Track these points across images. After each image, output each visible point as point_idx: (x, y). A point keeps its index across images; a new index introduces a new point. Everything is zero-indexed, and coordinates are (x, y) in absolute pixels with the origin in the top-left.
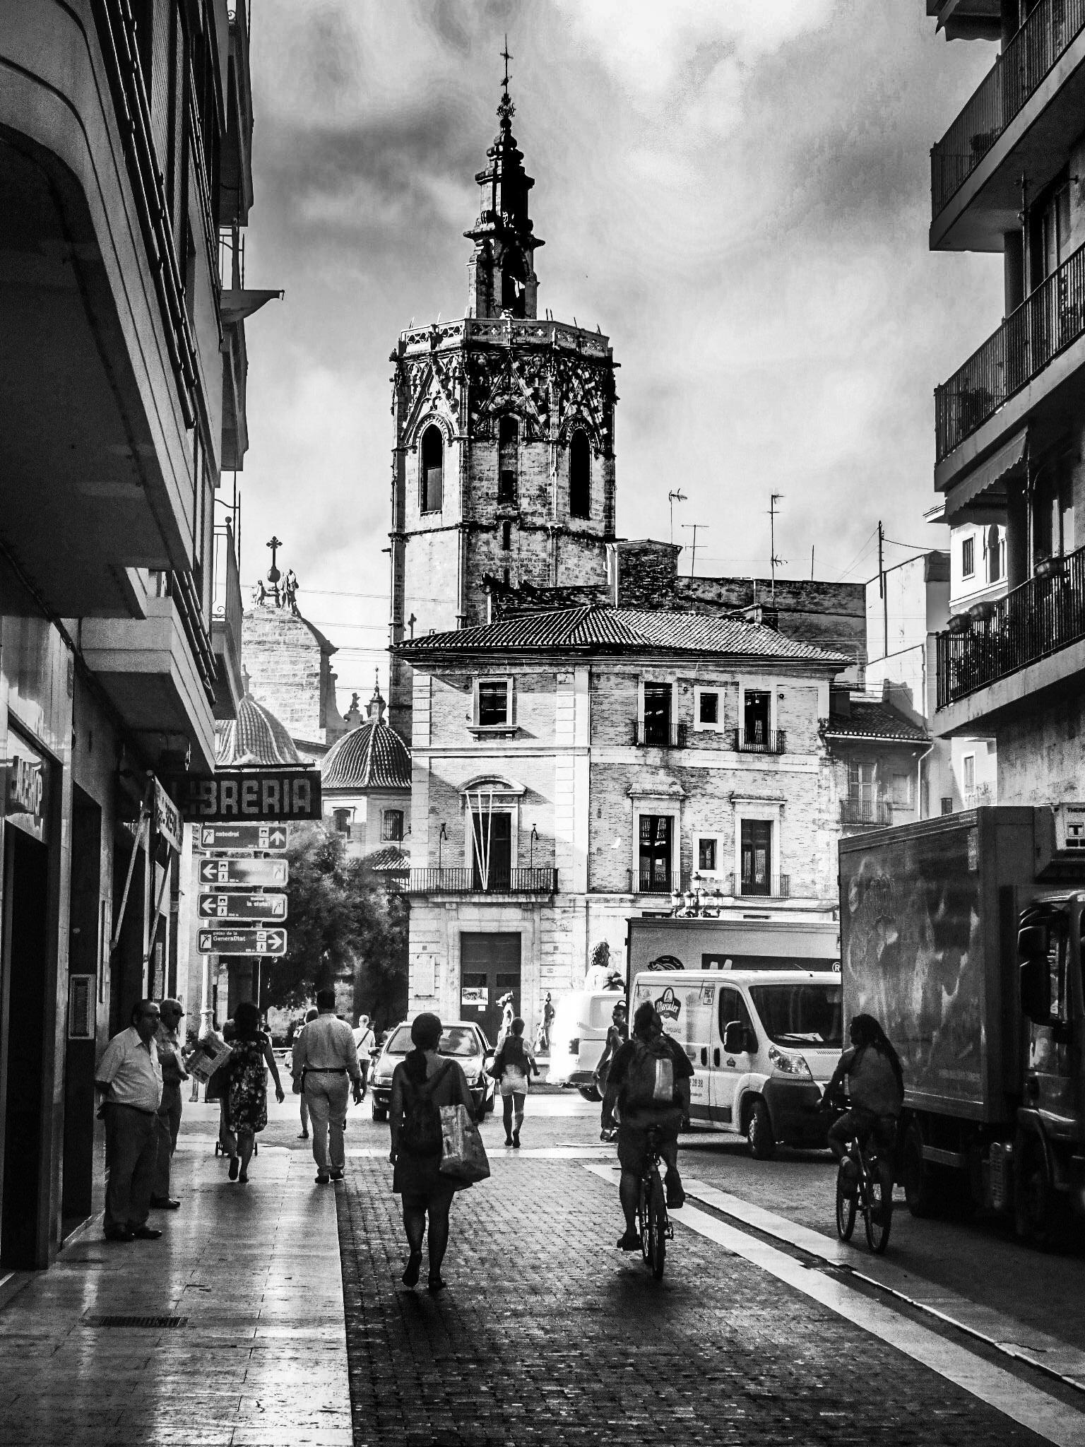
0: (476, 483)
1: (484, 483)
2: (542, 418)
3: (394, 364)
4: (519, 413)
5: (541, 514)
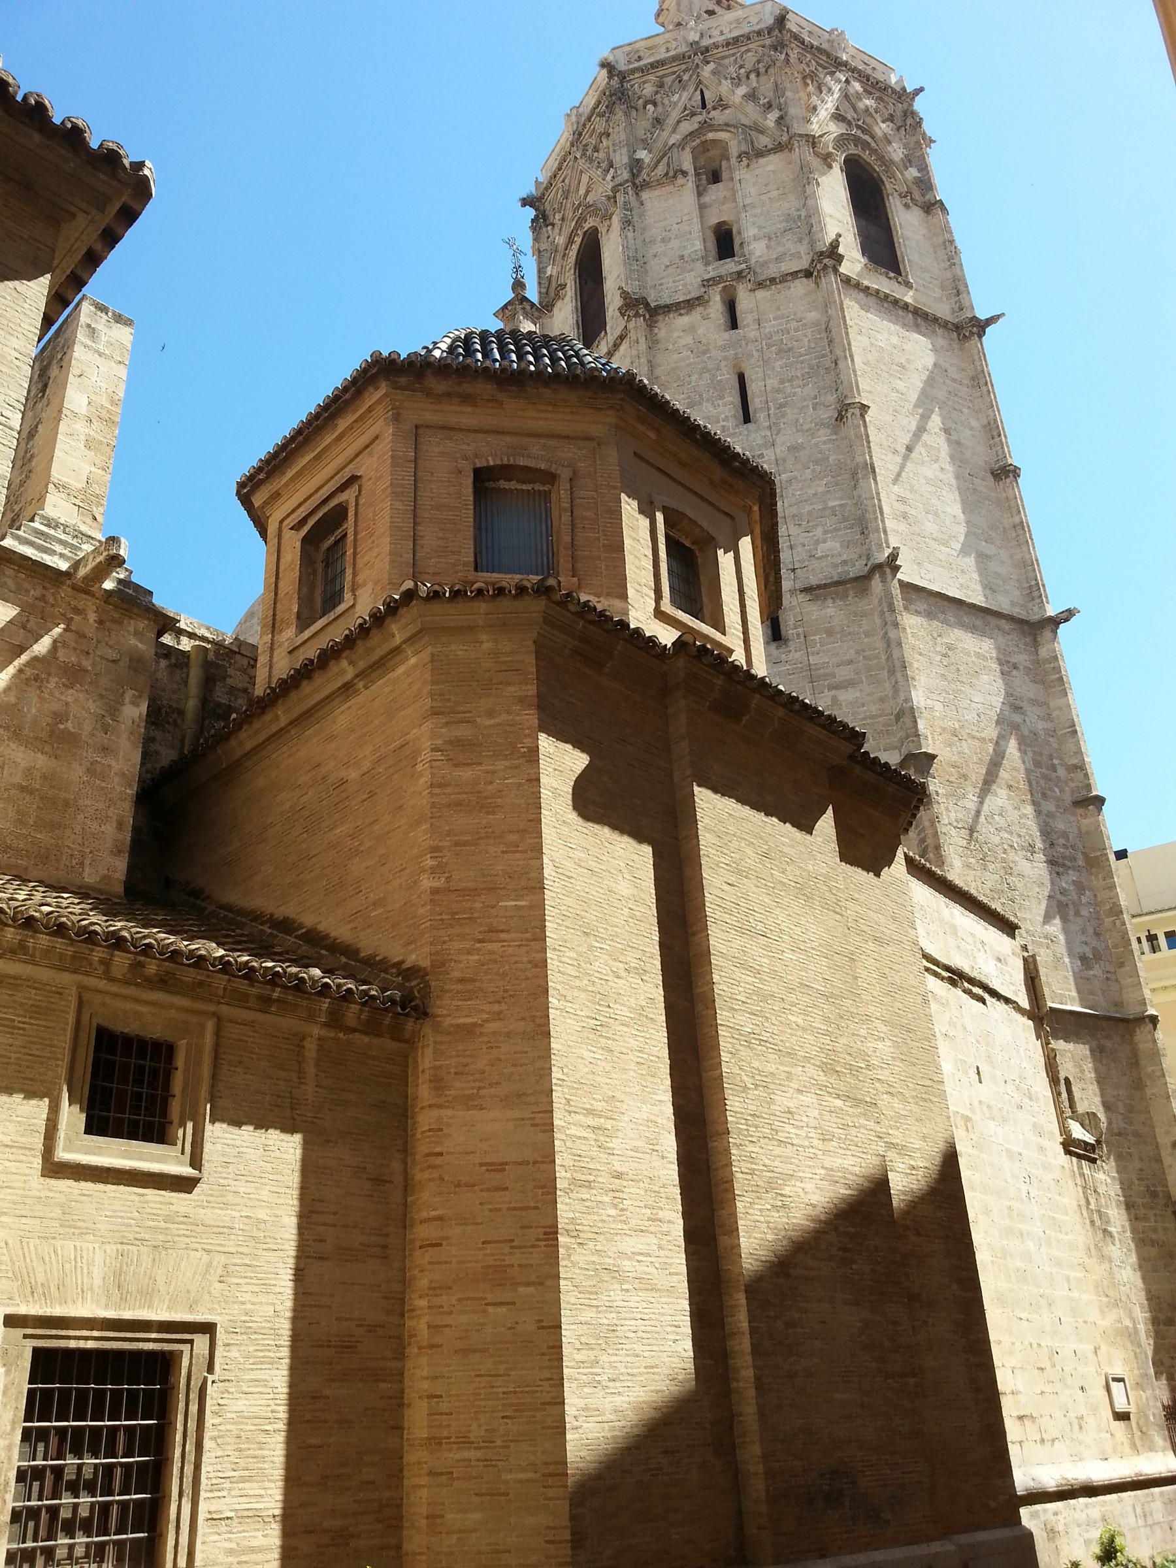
1: (674, 243)
3: (530, 212)
5: (797, 256)
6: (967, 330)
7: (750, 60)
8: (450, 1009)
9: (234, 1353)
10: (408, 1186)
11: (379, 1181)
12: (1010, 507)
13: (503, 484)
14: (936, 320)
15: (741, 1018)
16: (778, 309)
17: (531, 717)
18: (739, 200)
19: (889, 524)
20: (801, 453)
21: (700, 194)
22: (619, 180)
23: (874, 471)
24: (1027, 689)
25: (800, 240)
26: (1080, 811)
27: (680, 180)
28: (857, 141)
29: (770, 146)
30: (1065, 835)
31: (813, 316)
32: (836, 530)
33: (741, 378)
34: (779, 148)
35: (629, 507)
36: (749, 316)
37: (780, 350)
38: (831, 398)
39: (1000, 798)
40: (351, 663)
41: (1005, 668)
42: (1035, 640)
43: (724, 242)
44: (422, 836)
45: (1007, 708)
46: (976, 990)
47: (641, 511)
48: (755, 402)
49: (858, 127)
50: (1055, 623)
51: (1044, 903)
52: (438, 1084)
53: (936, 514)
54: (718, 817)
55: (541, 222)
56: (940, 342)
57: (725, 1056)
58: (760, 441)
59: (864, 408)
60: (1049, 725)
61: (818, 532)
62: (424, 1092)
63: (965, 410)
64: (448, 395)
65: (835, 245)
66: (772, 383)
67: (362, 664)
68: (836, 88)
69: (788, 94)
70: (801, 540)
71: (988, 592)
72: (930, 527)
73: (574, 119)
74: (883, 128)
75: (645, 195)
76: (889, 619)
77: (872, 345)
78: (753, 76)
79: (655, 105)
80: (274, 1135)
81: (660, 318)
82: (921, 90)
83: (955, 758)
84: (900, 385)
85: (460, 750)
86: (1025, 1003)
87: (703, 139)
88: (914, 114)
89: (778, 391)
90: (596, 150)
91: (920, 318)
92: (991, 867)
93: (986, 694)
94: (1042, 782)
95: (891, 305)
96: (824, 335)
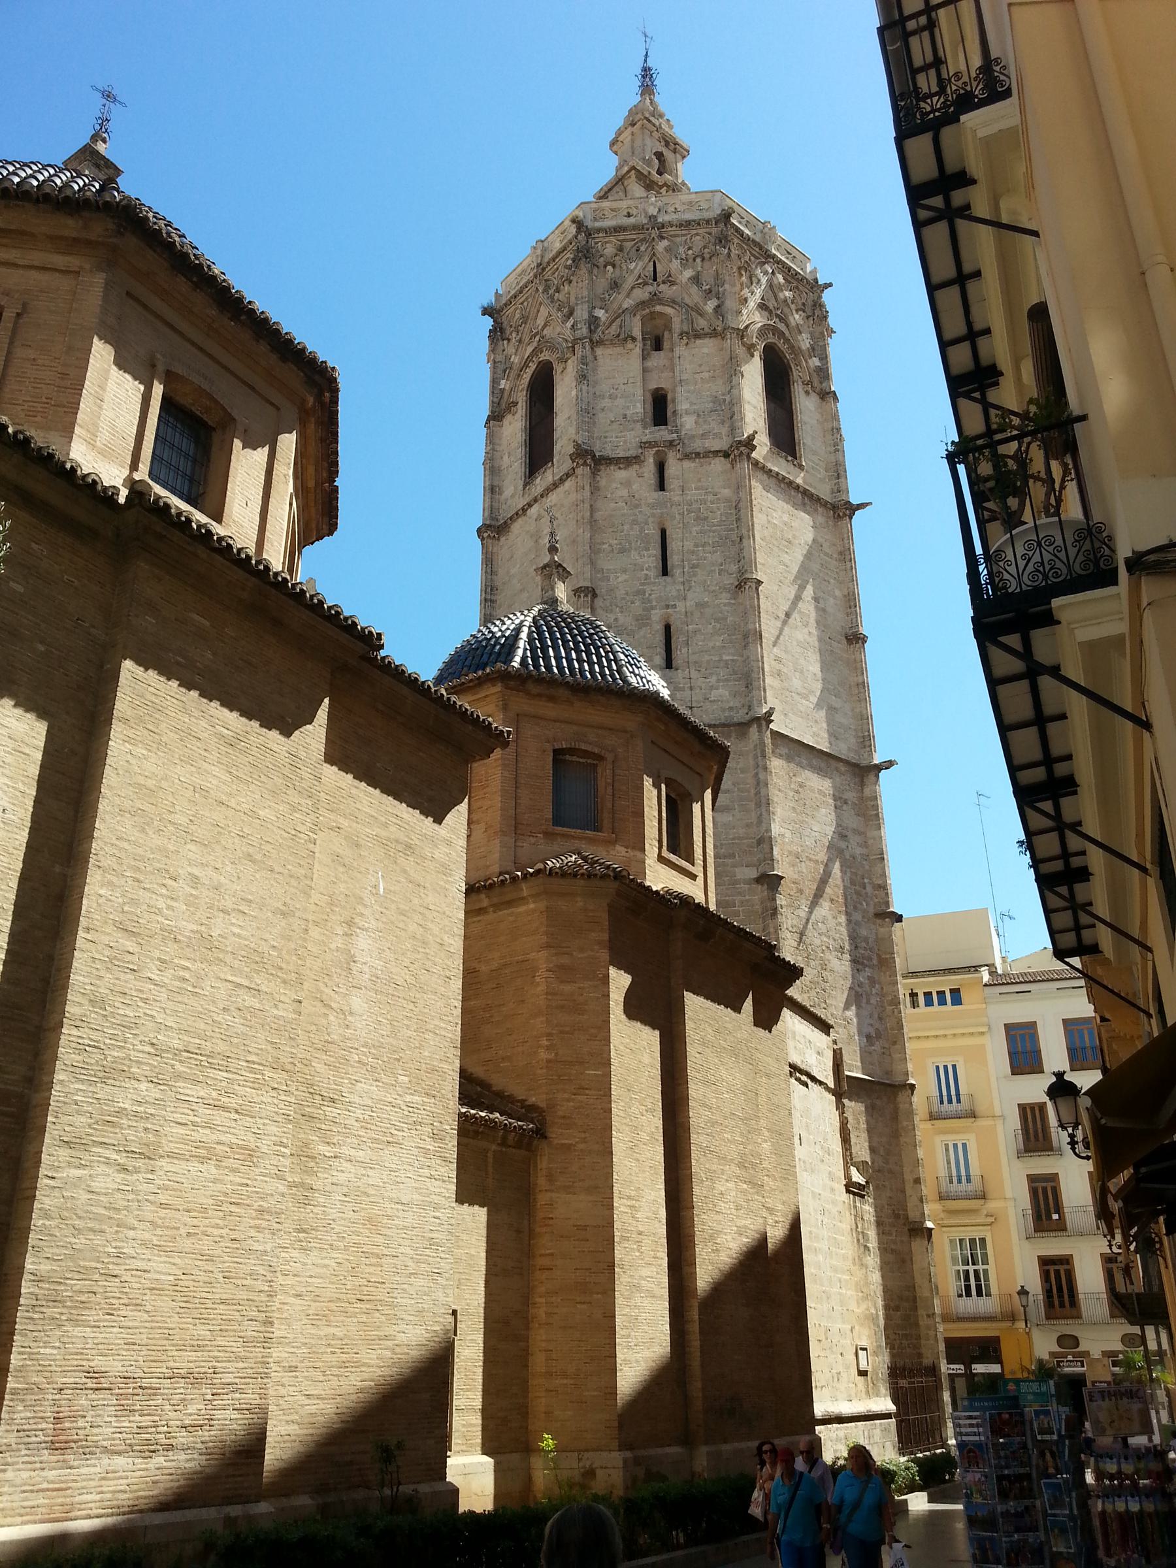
0: (606, 403)
1: (620, 402)
2: (710, 306)
3: (489, 322)
4: (673, 302)
5: (718, 436)
6: (841, 511)
7: (698, 242)
8: (558, 1135)
9: (463, 1326)
10: (531, 1234)
11: (518, 1231)
12: (856, 668)
13: (568, 757)
14: (819, 499)
15: (702, 1138)
16: (699, 480)
17: (605, 955)
18: (677, 374)
19: (769, 680)
20: (707, 610)
21: (644, 358)
22: (578, 334)
23: (761, 638)
24: (852, 821)
25: (723, 422)
26: (879, 921)
27: (630, 345)
28: (775, 330)
29: (707, 330)
30: (866, 940)
31: (726, 492)
32: (727, 680)
33: (663, 533)
34: (714, 334)
35: (648, 782)
36: (676, 482)
37: (697, 519)
38: (734, 568)
39: (824, 910)
40: (488, 897)
41: (839, 803)
42: (862, 781)
43: (660, 408)
44: (539, 1023)
45: (836, 836)
46: (804, 1078)
47: (654, 785)
48: (674, 559)
49: (777, 316)
50: (878, 768)
51: (846, 993)
52: (550, 1177)
53: (802, 672)
54: (695, 1006)
55: (497, 334)
56: (820, 519)
57: (694, 1162)
58: (674, 593)
59: (759, 583)
60: (864, 851)
61: (714, 678)
62: (542, 1182)
63: (832, 581)
64: (540, 695)
65: (751, 438)
66: (689, 545)
67: (495, 900)
68: (764, 280)
69: (727, 286)
70: (699, 684)
71: (833, 739)
72: (796, 683)
73: (539, 252)
74: (797, 318)
75: (599, 351)
76: (760, 763)
77: (769, 522)
78: (698, 260)
79: (614, 266)
80: (476, 1207)
81: (602, 467)
82: (830, 285)
83: (796, 876)
84: (786, 558)
85: (564, 972)
86: (831, 1085)
87: (652, 309)
88: (822, 306)
89: (693, 552)
90: (558, 291)
91: (806, 498)
92: (812, 963)
93: (822, 824)
94: (855, 897)
95: (786, 486)
96: (733, 511)
